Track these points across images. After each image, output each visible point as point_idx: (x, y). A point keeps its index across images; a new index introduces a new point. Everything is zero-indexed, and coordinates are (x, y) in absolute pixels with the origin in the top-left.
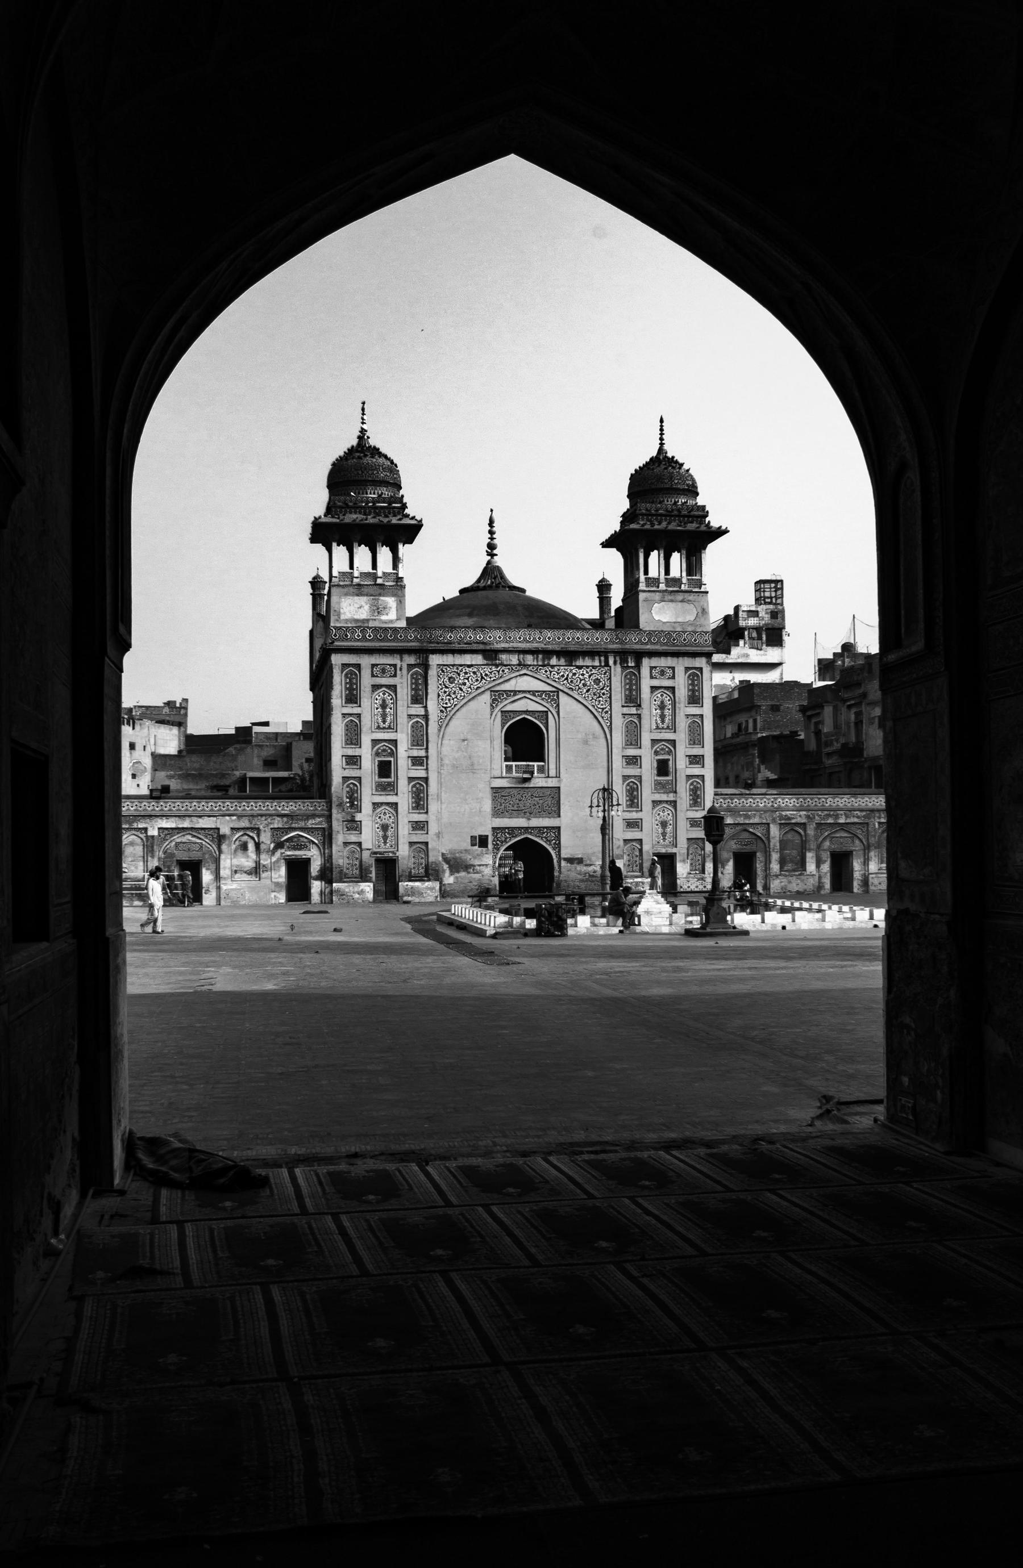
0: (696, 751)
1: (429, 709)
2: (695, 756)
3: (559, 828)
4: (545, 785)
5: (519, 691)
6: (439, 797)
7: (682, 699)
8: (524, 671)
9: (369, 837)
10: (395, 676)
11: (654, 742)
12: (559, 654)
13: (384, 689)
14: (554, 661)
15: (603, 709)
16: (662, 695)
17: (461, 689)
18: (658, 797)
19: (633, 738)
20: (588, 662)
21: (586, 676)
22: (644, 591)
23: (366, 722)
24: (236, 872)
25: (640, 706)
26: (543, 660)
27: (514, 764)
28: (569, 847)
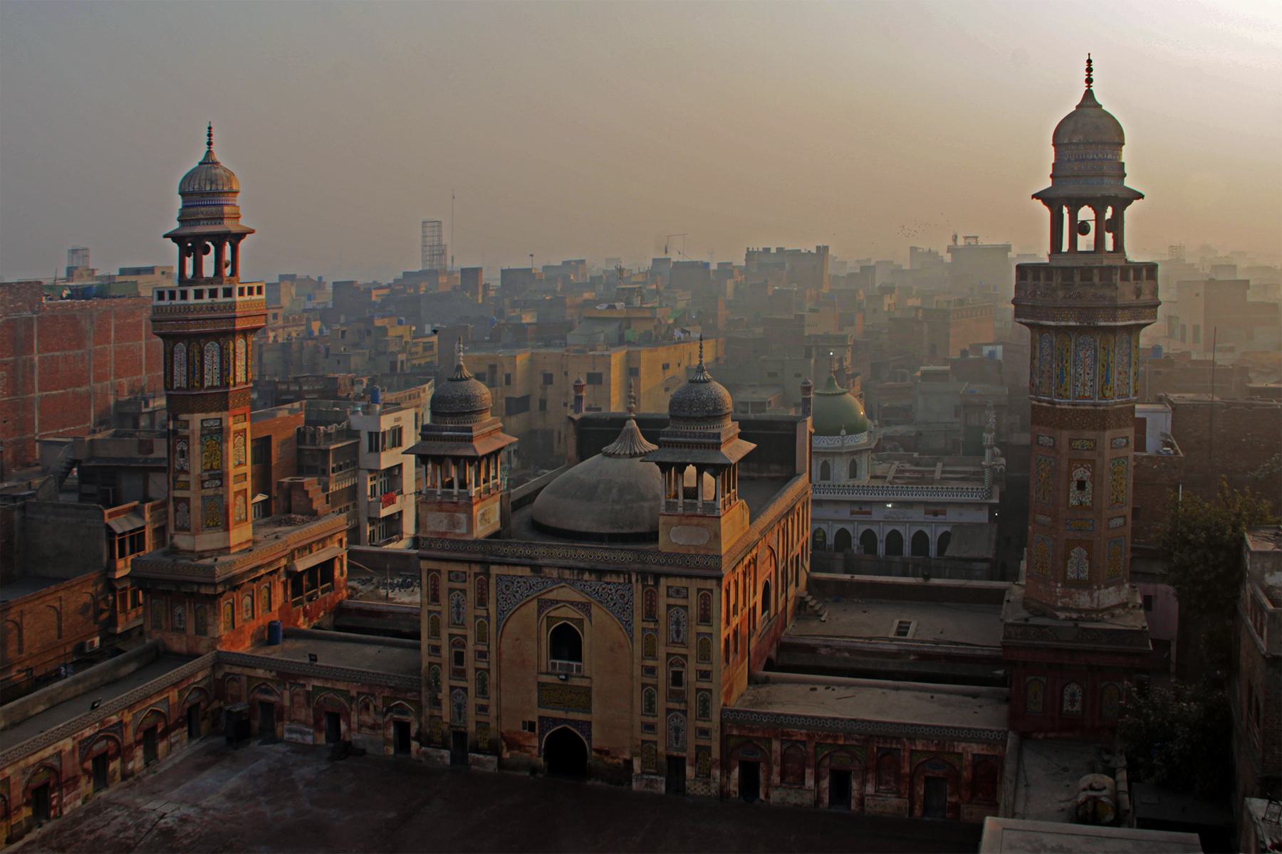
0: (704, 667)
1: (491, 611)
2: (705, 671)
3: (589, 723)
4: (579, 684)
5: (561, 601)
6: (498, 687)
7: (695, 618)
8: (563, 584)
9: (446, 711)
10: (465, 581)
11: (669, 655)
12: (591, 571)
13: (457, 592)
14: (586, 576)
15: (627, 622)
16: (678, 613)
17: (514, 596)
18: (671, 705)
19: (650, 652)
20: (614, 579)
21: (613, 591)
22: (664, 515)
23: (444, 619)
24: (362, 726)
25: (657, 621)
26: (578, 575)
27: (558, 662)
28: (597, 739)
